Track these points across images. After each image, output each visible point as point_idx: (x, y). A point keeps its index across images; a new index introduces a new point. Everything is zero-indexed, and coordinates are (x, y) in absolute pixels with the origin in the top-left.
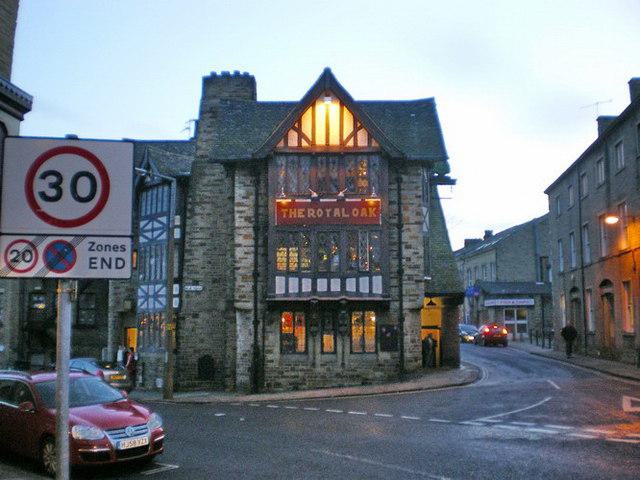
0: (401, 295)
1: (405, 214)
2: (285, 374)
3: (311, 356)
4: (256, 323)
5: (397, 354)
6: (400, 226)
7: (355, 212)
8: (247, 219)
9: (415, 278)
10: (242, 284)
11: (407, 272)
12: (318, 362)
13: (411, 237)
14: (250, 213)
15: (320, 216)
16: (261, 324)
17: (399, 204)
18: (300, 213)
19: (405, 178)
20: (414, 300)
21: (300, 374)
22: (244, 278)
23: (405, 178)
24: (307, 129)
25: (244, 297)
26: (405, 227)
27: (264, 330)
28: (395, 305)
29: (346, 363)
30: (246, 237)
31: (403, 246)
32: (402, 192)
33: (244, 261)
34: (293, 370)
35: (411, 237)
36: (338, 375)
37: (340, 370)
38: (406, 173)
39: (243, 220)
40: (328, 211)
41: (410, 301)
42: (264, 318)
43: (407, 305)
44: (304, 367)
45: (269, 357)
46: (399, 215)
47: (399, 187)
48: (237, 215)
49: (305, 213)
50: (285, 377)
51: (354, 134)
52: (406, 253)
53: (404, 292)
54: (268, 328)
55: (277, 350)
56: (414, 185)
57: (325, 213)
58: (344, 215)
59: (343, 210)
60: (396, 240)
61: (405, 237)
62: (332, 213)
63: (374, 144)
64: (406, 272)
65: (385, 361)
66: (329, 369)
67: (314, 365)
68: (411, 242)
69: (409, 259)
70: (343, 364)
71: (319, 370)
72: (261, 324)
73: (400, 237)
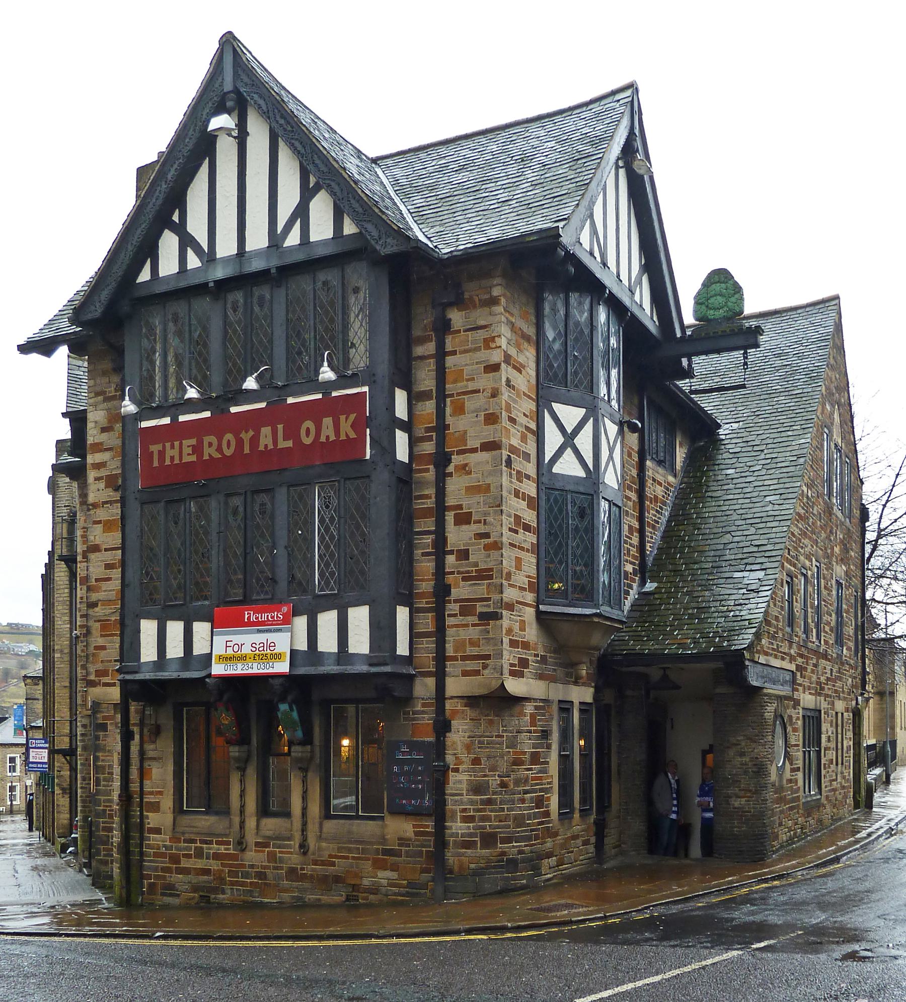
0: (441, 658)
1: (456, 424)
2: (185, 863)
3: (236, 820)
4: (127, 737)
5: (429, 825)
6: (442, 460)
7: (307, 432)
8: (110, 481)
9: (480, 608)
10: (101, 641)
11: (460, 590)
12: (251, 838)
13: (472, 490)
14: (114, 466)
15: (228, 452)
16: (137, 737)
17: (442, 396)
18: (187, 450)
19: (456, 317)
20: (477, 673)
21: (214, 865)
22: (105, 625)
23: (456, 317)
24: (197, 227)
25: (104, 673)
26: (456, 460)
27: (142, 753)
28: (424, 688)
29: (312, 842)
30: (108, 526)
31: (450, 517)
32: (450, 361)
33: (104, 585)
34: (199, 854)
35: (472, 490)
36: (292, 873)
37: (294, 859)
38: (459, 302)
39: (102, 485)
40: (246, 436)
41: (465, 673)
42: (142, 724)
43: (455, 686)
44: (222, 849)
45: (153, 819)
46: (441, 427)
47: (441, 345)
48: (91, 475)
49: (197, 449)
50: (185, 871)
51: (302, 213)
52: (456, 536)
53: (450, 651)
54: (149, 747)
55: (167, 803)
56: (481, 334)
57: (240, 443)
58: (283, 444)
59: (280, 427)
60: (430, 503)
61: (455, 487)
62: (255, 441)
63: (349, 228)
64: (455, 593)
65: (403, 841)
66: (272, 857)
67: (241, 844)
68: (474, 504)
69: (464, 555)
70: (304, 846)
71: (253, 857)
72: (137, 737)
73: (441, 493)
